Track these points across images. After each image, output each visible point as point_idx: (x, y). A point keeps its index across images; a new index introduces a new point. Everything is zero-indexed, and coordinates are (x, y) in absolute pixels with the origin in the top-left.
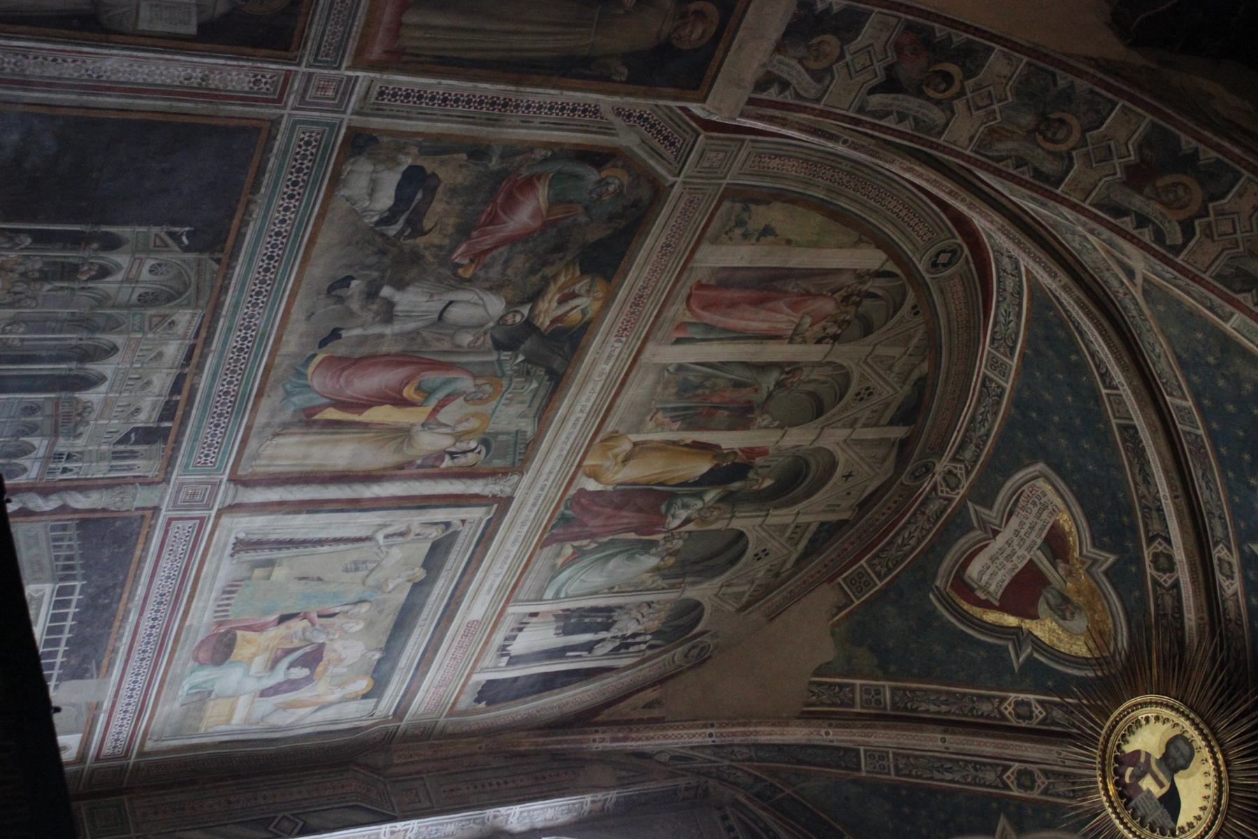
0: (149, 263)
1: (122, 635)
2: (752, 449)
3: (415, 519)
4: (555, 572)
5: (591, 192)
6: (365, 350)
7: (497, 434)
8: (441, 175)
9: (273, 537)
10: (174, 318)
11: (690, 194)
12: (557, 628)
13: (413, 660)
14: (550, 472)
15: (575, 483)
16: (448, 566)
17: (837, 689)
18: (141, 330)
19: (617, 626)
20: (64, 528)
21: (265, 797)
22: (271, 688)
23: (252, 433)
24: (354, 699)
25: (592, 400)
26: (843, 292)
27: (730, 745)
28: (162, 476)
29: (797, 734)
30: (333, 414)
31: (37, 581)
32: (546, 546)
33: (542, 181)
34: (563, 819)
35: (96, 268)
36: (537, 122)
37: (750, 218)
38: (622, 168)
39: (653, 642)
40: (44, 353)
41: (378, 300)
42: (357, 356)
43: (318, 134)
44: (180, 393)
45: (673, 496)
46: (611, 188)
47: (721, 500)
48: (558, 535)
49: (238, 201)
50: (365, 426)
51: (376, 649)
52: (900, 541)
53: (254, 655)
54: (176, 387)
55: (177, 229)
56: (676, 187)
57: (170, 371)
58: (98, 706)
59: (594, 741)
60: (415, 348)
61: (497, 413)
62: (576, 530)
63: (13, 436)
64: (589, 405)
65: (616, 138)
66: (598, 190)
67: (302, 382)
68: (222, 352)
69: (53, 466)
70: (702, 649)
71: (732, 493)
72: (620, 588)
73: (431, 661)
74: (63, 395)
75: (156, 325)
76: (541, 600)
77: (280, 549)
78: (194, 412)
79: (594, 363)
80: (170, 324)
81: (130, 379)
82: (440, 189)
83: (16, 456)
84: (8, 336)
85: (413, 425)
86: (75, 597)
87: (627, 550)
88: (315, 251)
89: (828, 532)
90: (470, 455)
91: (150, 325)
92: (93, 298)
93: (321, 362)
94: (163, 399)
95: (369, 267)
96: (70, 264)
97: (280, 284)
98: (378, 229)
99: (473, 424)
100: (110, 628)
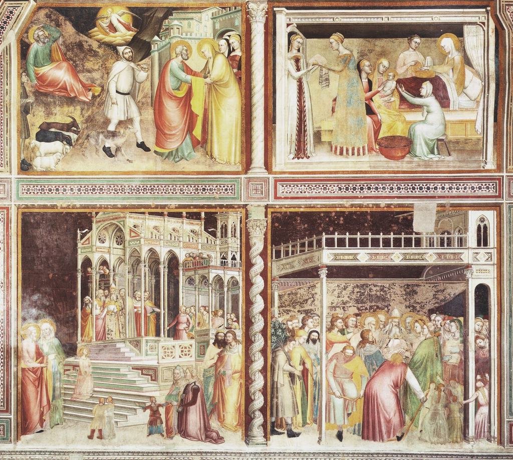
0: (99, 244)
10: (132, 227)
30: (198, 132)
33: (39, 72)
35: (102, 267)
40: (154, 281)
41: (117, 130)
44: (182, 213)
46: (41, 33)
49: (63, 213)
54: (178, 215)
65: (12, 44)
66: (42, 40)
74: (181, 268)
75: (136, 233)
77: (305, 131)
80: (135, 227)
83: (223, 283)
91: (137, 236)
93: (161, 147)
94: (185, 221)
95: (97, 141)
96: (100, 278)
98: (74, 144)
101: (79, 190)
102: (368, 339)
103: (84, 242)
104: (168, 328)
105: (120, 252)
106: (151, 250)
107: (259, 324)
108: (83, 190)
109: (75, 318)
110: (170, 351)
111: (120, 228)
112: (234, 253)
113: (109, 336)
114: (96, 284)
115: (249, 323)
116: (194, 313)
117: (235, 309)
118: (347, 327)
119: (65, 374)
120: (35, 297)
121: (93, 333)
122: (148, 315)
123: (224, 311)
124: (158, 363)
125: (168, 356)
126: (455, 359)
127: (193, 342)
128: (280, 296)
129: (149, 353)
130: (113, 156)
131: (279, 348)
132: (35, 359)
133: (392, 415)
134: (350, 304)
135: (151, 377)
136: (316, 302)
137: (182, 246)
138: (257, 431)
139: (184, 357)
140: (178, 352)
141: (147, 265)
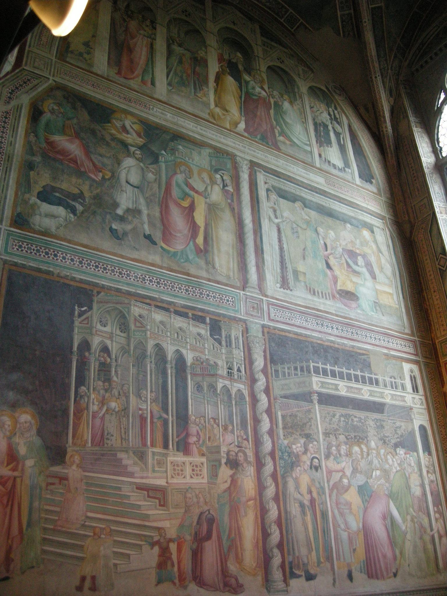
0: (99, 327)
1: (344, 343)
2: (219, 60)
3: (265, 206)
4: (293, 144)
5: (57, 116)
6: (159, 224)
7: (212, 166)
8: (44, 184)
9: (279, 271)
11: (60, 74)
12: (328, 147)
13: (351, 210)
14: (234, 143)
15: (241, 133)
16: (294, 191)
17: (344, 23)
18: (145, 332)
19: (325, 121)
20: (277, 371)
21: (430, 275)
22: (370, 274)
23: (213, 279)
24: (374, 237)
25: (189, 122)
26: (126, 17)
27: (380, 70)
28: (242, 323)
29: (369, 37)
30: (200, 240)
31: (311, 384)
32: (279, 147)
34: (426, 139)
35: (102, 354)
36: (11, 139)
37: (77, 50)
38: (43, 102)
39: (333, 108)
40: (161, 381)
41: (126, 216)
42: (162, 227)
43: (14, 241)
44: (188, 313)
45: (247, 94)
46: (56, 108)
47: (249, 74)
48: (272, 142)
49: (58, 282)
50: (207, 226)
51: (345, 227)
52: (268, 4)
53: (351, 281)
55: (76, 313)
56: (56, 80)
57: (172, 318)
58: (386, 355)
59: (387, 131)
60: (157, 200)
61: (198, 164)
62: (269, 134)
63: (217, 397)
64: (192, 124)
67: (179, 254)
68: (160, 292)
69: (236, 377)
70: (335, 88)
71: (245, 69)
72: (302, 119)
73: (350, 202)
74: (188, 371)
76: (311, 152)
77: (286, 268)
78: (199, 307)
79: (166, 120)
80: (141, 318)
81: (178, 337)
82: (53, 184)
83: (230, 396)
84: (149, 399)
85: (206, 203)
86: (320, 365)
87: (281, 115)
88: (93, 245)
89: (265, 33)
90: (225, 178)
91: (142, 327)
92: (123, 355)
94: (191, 322)
95: (104, 220)
96: (99, 367)
97: (114, 262)
98: (78, 215)
99: (205, 176)
100: (338, 349)
101: (81, 262)
102: (357, 469)
103: (83, 321)
104: (177, 440)
105: (123, 341)
106: (157, 345)
107: (267, 445)
108: (85, 264)
109: (65, 412)
110: (179, 468)
111: (124, 314)
112: (238, 365)
113: (109, 442)
114: (94, 373)
115: (258, 443)
116: (204, 424)
117: (244, 424)
118: (340, 455)
119: (47, 490)
120: (15, 376)
121: (88, 435)
122: (155, 420)
123: (233, 426)
124: (167, 483)
125: (178, 474)
126: (417, 491)
127: (204, 460)
128: (283, 417)
129: (156, 469)
130: (120, 239)
131: (288, 474)
132: (5, 464)
133: (386, 548)
134: (340, 432)
135: (160, 502)
136: (313, 427)
137: (189, 347)
138: (277, 575)
139: (195, 477)
140: (188, 470)
141: (153, 362)
